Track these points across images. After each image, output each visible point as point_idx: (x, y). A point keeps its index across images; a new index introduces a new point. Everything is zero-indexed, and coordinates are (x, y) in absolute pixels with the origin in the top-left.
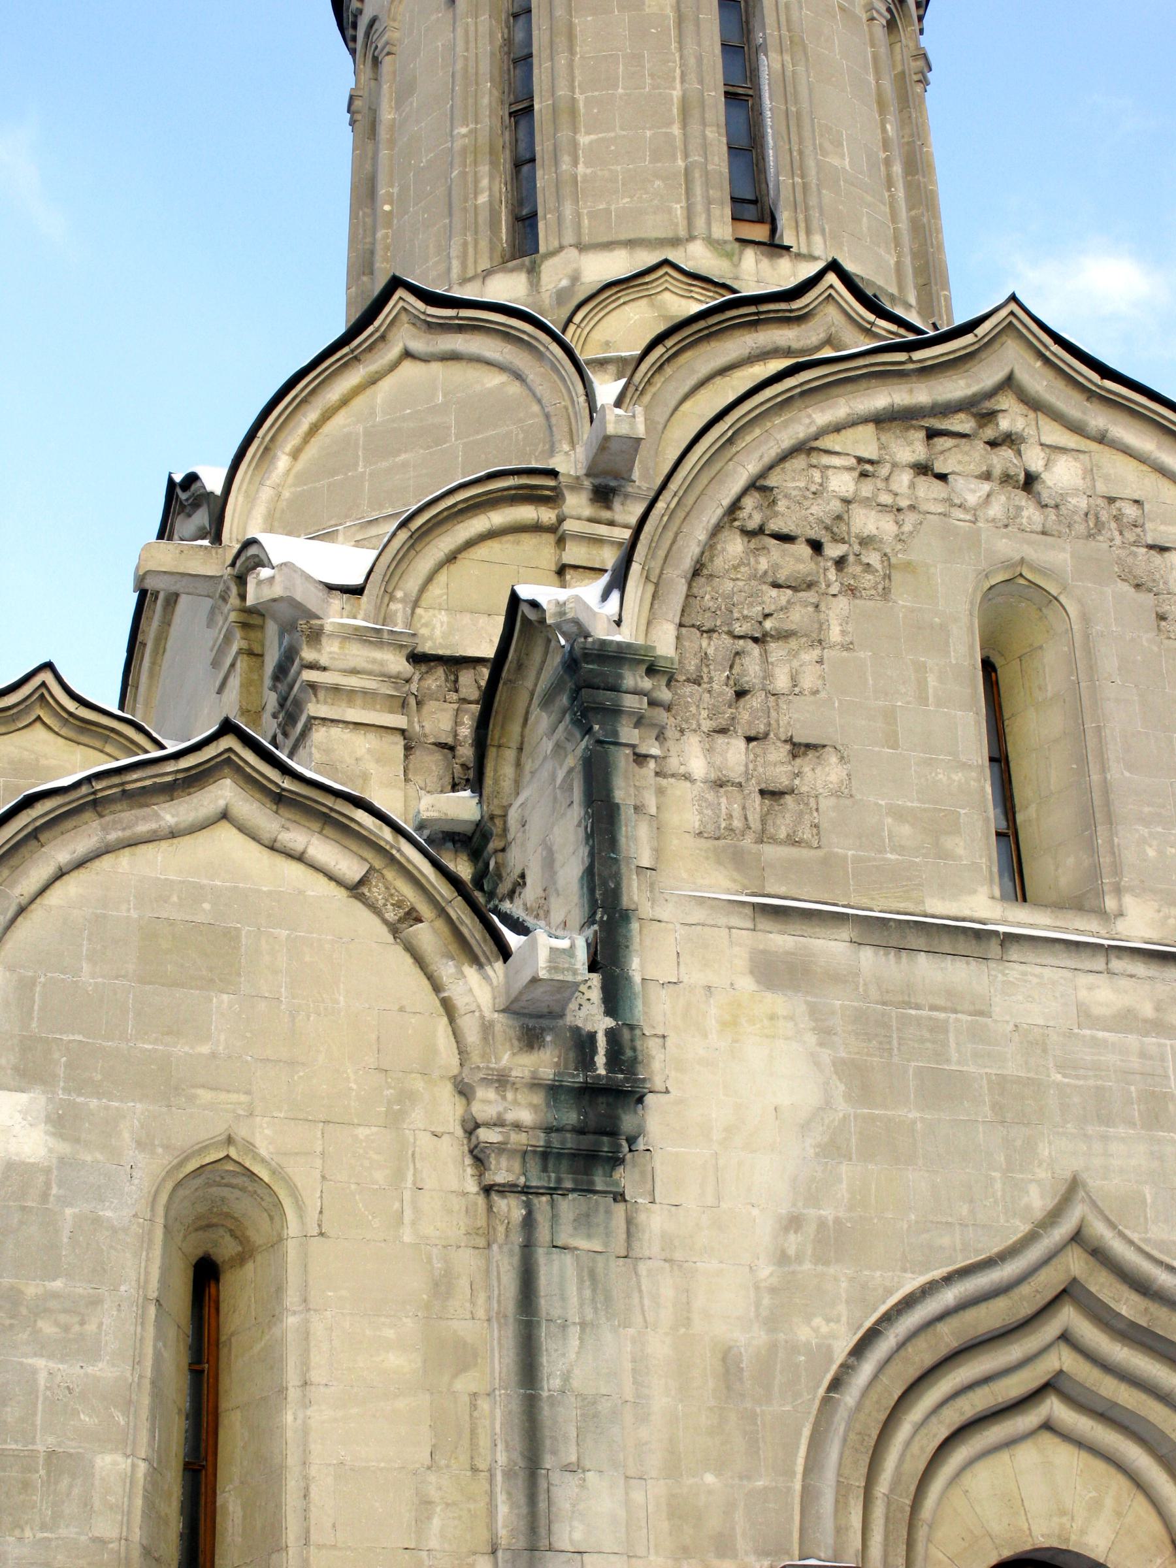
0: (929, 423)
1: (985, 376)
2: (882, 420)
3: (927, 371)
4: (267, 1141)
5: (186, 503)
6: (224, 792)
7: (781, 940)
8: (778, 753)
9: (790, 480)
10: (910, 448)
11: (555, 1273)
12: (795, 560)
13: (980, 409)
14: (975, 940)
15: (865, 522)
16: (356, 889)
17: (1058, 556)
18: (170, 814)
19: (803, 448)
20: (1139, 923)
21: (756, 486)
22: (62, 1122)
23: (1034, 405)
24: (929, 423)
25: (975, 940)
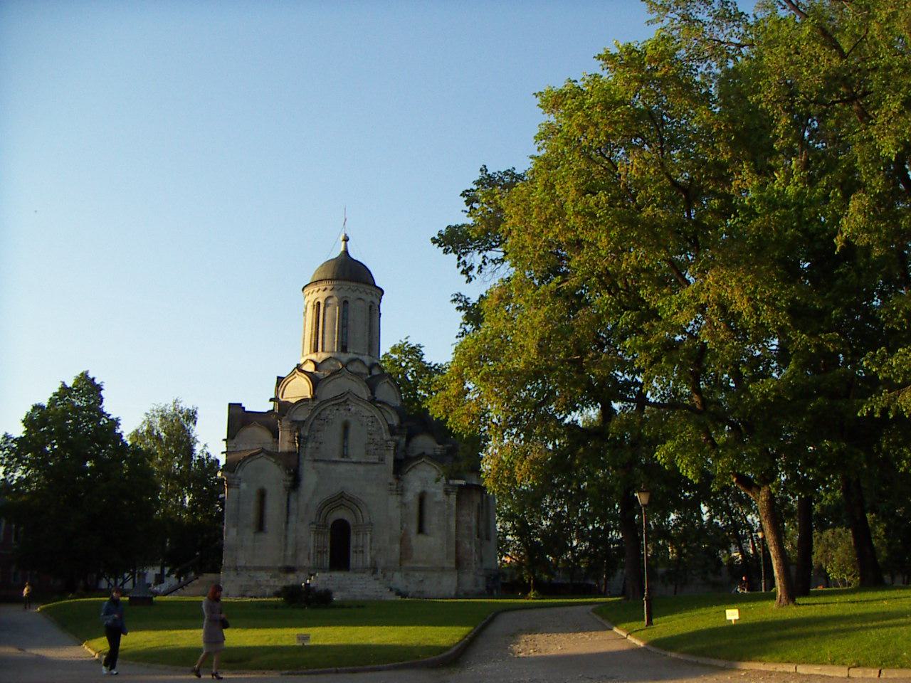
0: (338, 404)
1: (346, 398)
2: (333, 405)
3: (340, 398)
4: (266, 487)
5: (280, 379)
6: (262, 454)
7: (316, 464)
8: (318, 444)
9: (323, 413)
10: (337, 407)
11: (292, 500)
12: (322, 422)
13: (345, 402)
14: (336, 462)
15: (331, 417)
16: (274, 462)
17: (349, 419)
18: (258, 456)
19: (324, 409)
20: (354, 460)
21: (319, 414)
22: (248, 486)
23: (351, 401)
24: (338, 404)
25: (336, 462)
